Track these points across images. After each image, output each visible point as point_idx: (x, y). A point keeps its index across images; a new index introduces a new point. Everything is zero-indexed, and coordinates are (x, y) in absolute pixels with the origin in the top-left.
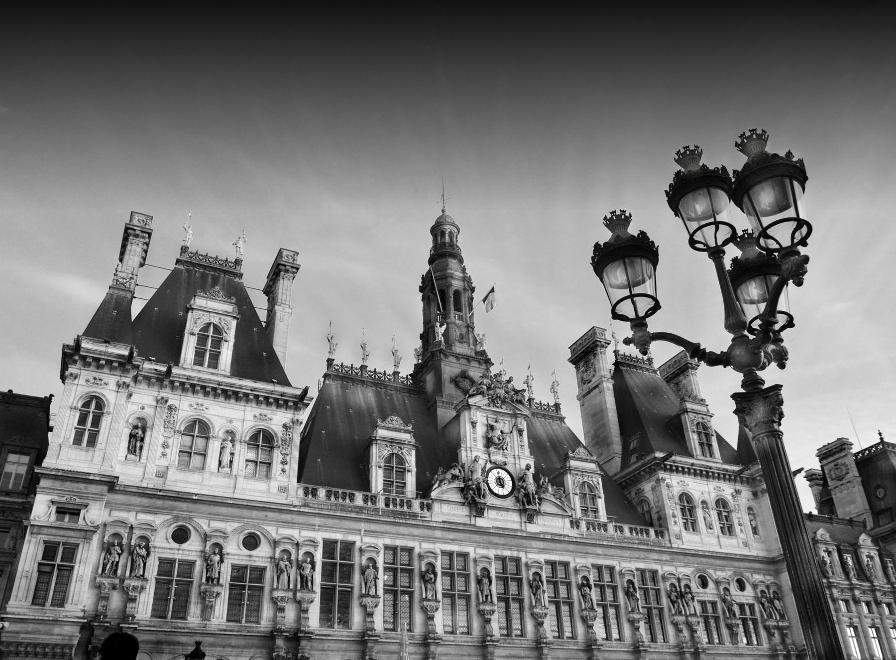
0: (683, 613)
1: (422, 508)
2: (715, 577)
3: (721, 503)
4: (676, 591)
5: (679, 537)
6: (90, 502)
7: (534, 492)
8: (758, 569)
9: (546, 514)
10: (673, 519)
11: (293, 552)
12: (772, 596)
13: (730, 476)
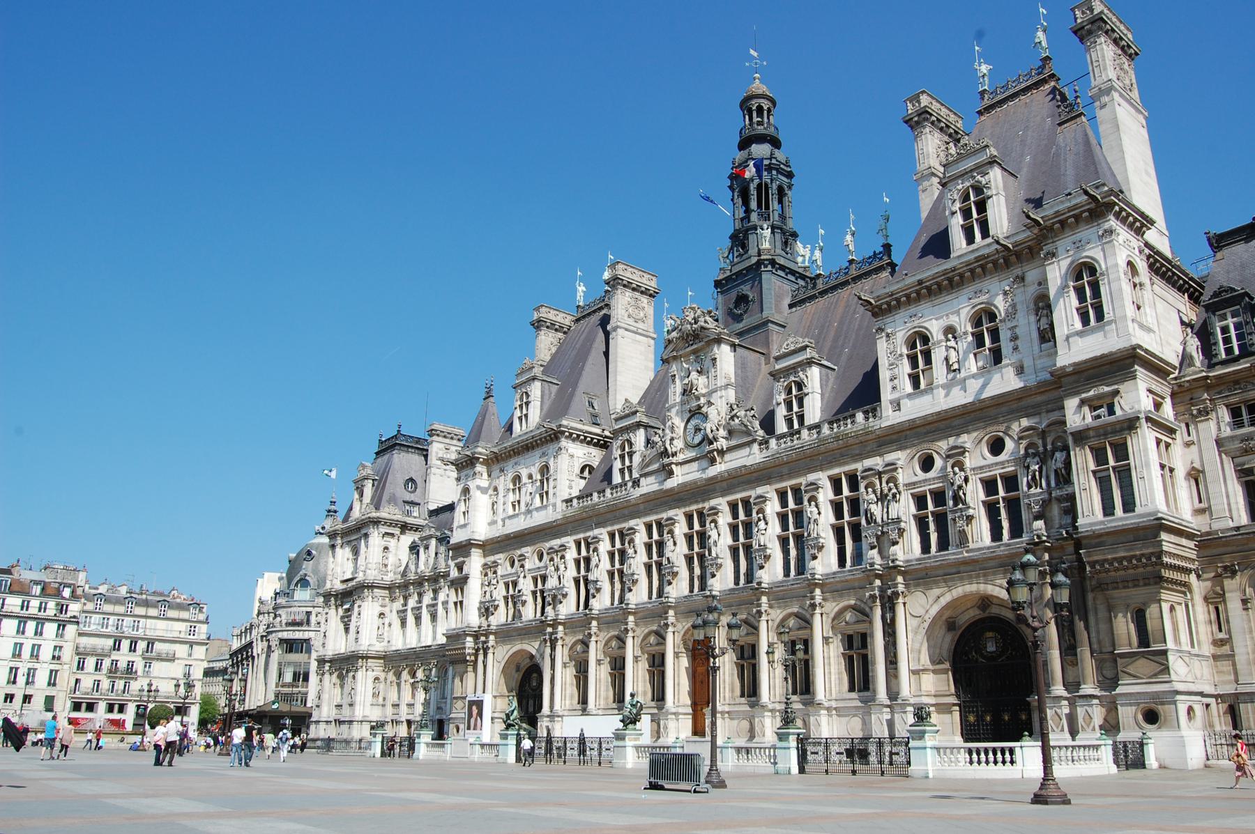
0: (879, 520)
1: (633, 486)
2: (945, 447)
3: (983, 317)
4: (874, 492)
5: (897, 405)
6: (465, 559)
7: (714, 428)
8: (1033, 407)
9: (730, 449)
10: (891, 384)
11: (555, 557)
12: (1049, 447)
13: (995, 263)
